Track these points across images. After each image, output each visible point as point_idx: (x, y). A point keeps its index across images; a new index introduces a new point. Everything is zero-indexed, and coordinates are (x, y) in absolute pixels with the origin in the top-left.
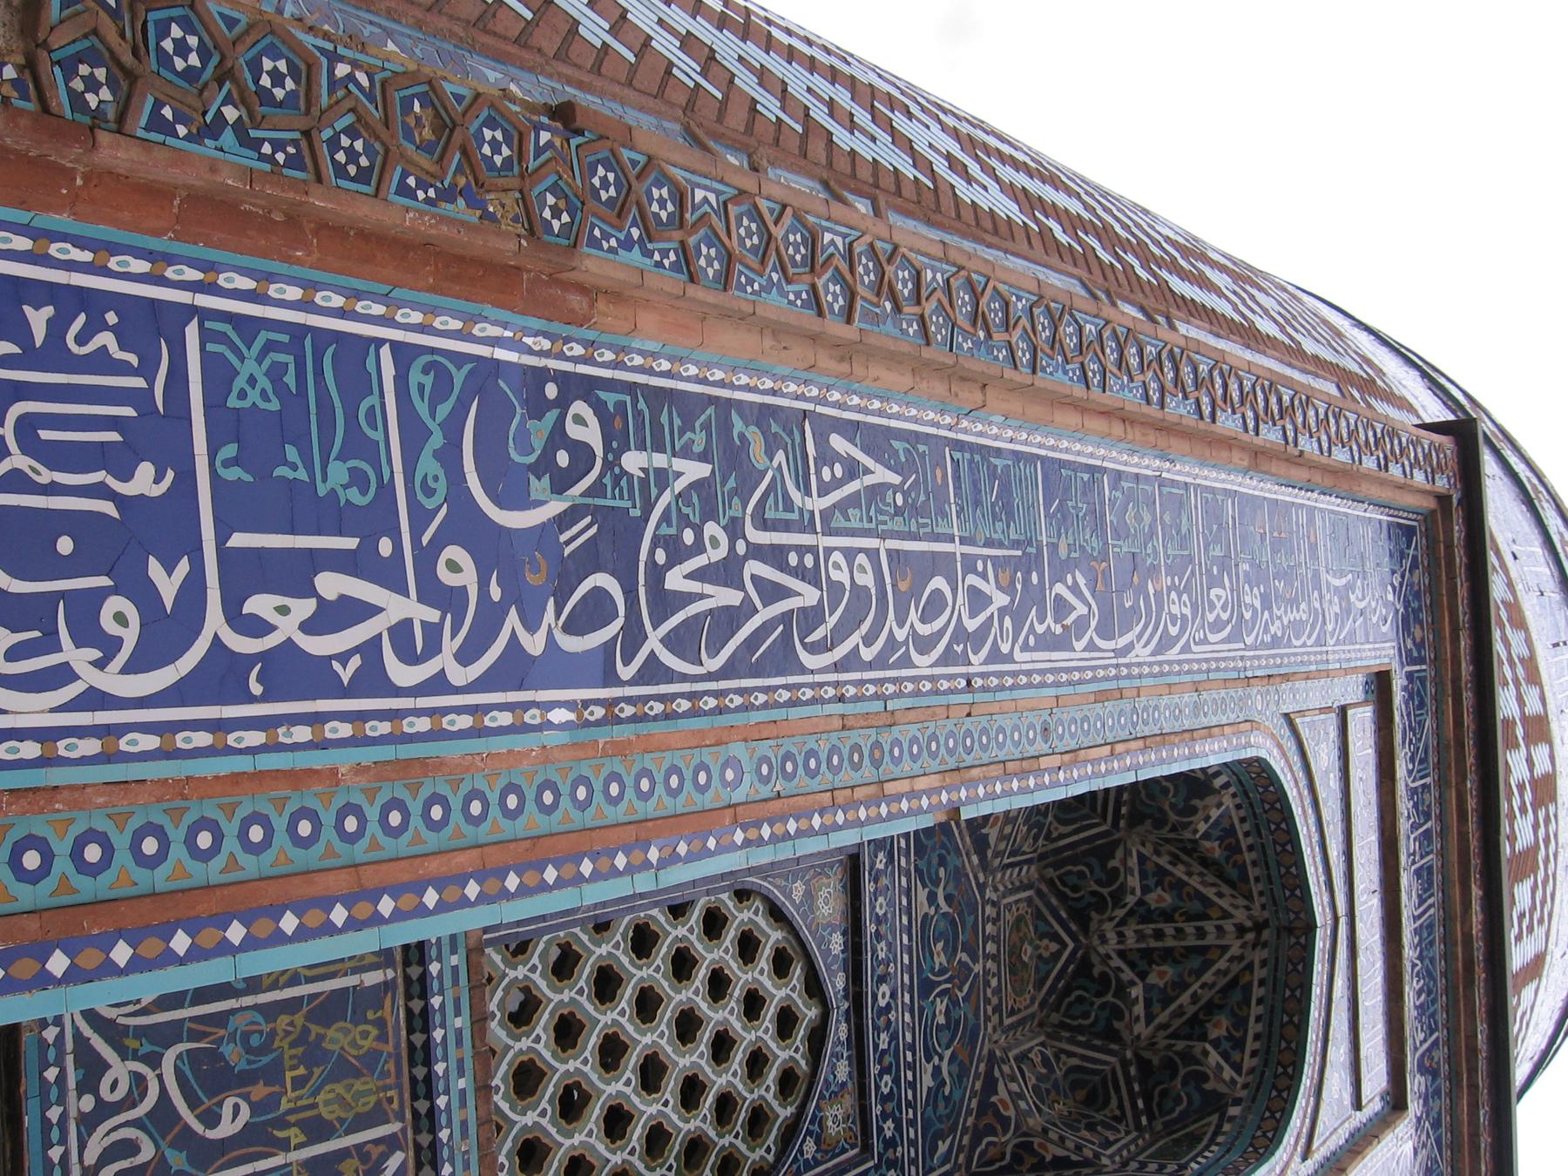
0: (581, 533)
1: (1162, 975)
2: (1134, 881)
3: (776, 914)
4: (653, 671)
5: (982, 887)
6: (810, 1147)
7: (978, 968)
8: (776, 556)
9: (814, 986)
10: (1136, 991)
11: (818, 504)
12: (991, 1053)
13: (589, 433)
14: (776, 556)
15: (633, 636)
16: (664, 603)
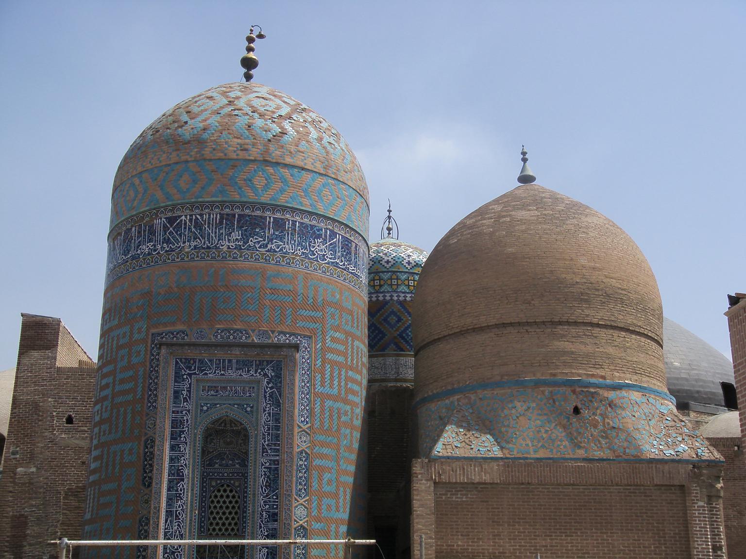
0: (172, 556)
1: (233, 425)
2: (220, 428)
3: (214, 492)
4: (181, 550)
5: (218, 451)
6: (239, 489)
7: (227, 452)
8: (175, 535)
9: (222, 486)
10: (235, 428)
11: (171, 530)
12: (239, 450)
13: (166, 555)
14: (175, 535)
15: (179, 552)
16: (177, 549)
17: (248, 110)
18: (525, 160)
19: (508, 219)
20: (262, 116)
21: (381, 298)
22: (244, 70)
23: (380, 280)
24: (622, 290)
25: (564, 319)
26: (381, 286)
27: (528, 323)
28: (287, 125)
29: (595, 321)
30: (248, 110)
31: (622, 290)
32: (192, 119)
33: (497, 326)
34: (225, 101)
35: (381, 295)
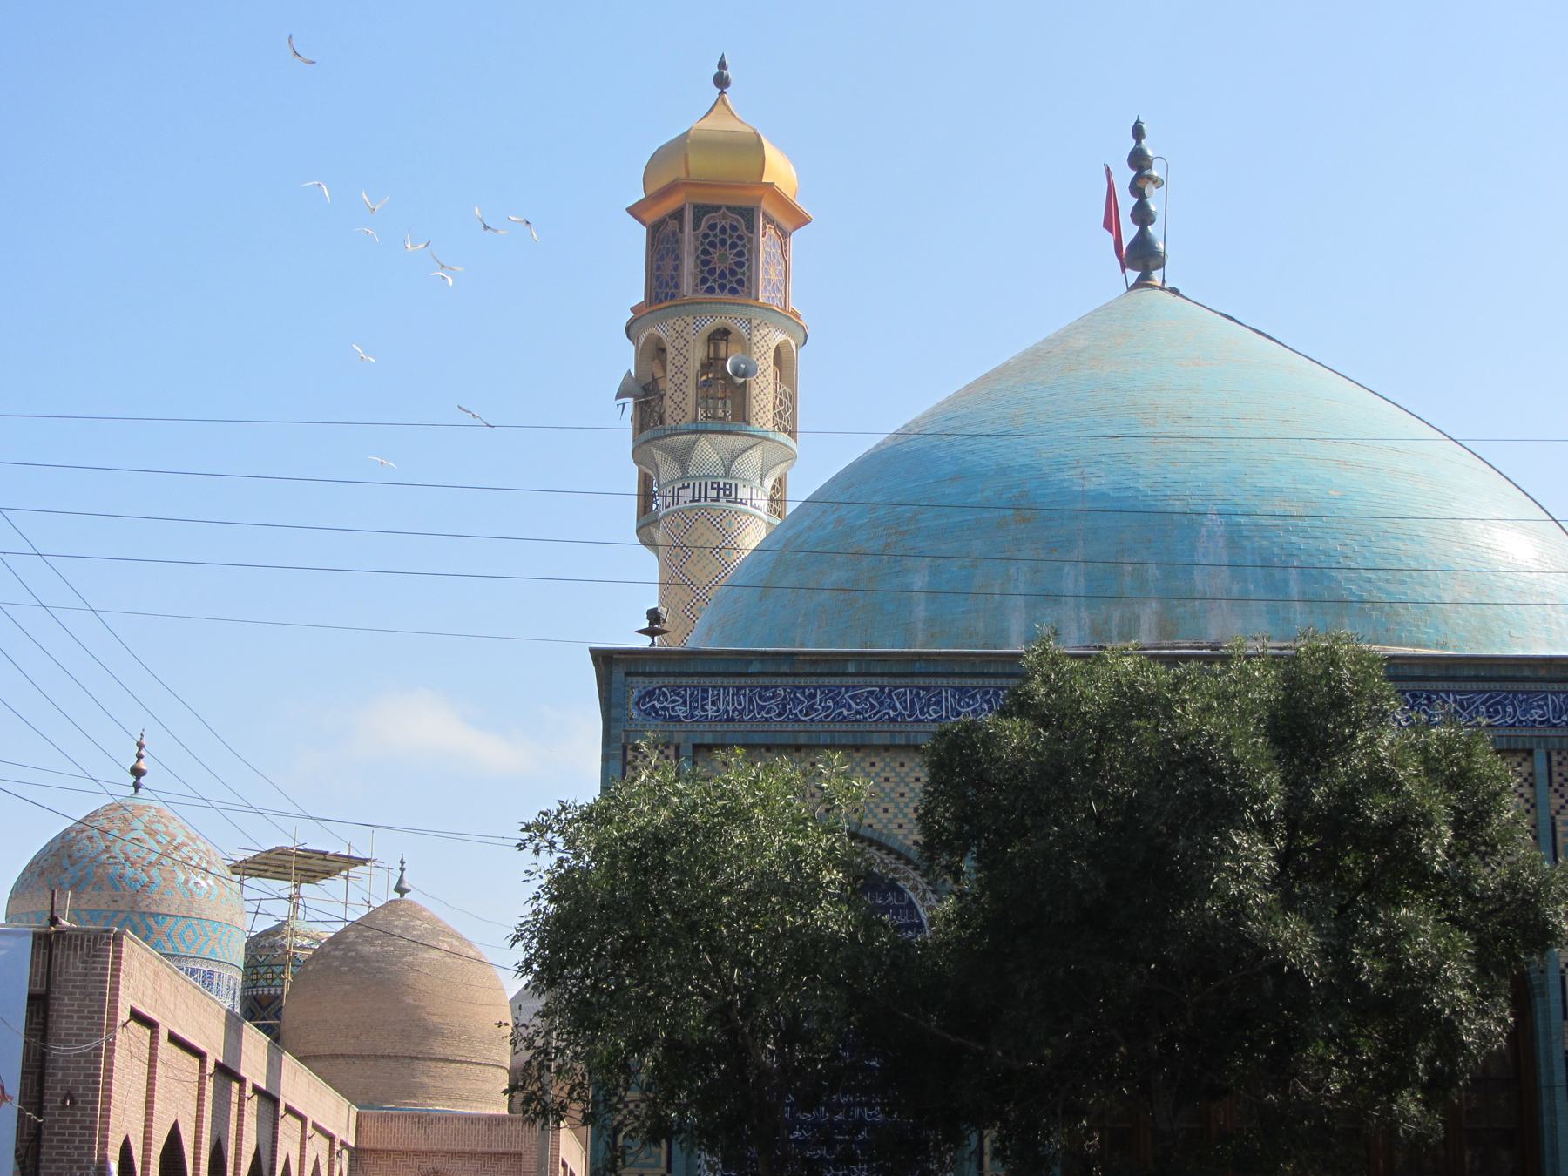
17: (121, 858)
18: (402, 870)
19: (353, 954)
20: (133, 864)
21: (273, 992)
22: (133, 779)
23: (272, 973)
24: (444, 1024)
25: (386, 1053)
26: (273, 979)
27: (355, 1056)
28: (154, 872)
29: (414, 1054)
30: (121, 858)
31: (444, 1024)
32: (72, 865)
33: (331, 1056)
34: (102, 845)
35: (273, 989)
